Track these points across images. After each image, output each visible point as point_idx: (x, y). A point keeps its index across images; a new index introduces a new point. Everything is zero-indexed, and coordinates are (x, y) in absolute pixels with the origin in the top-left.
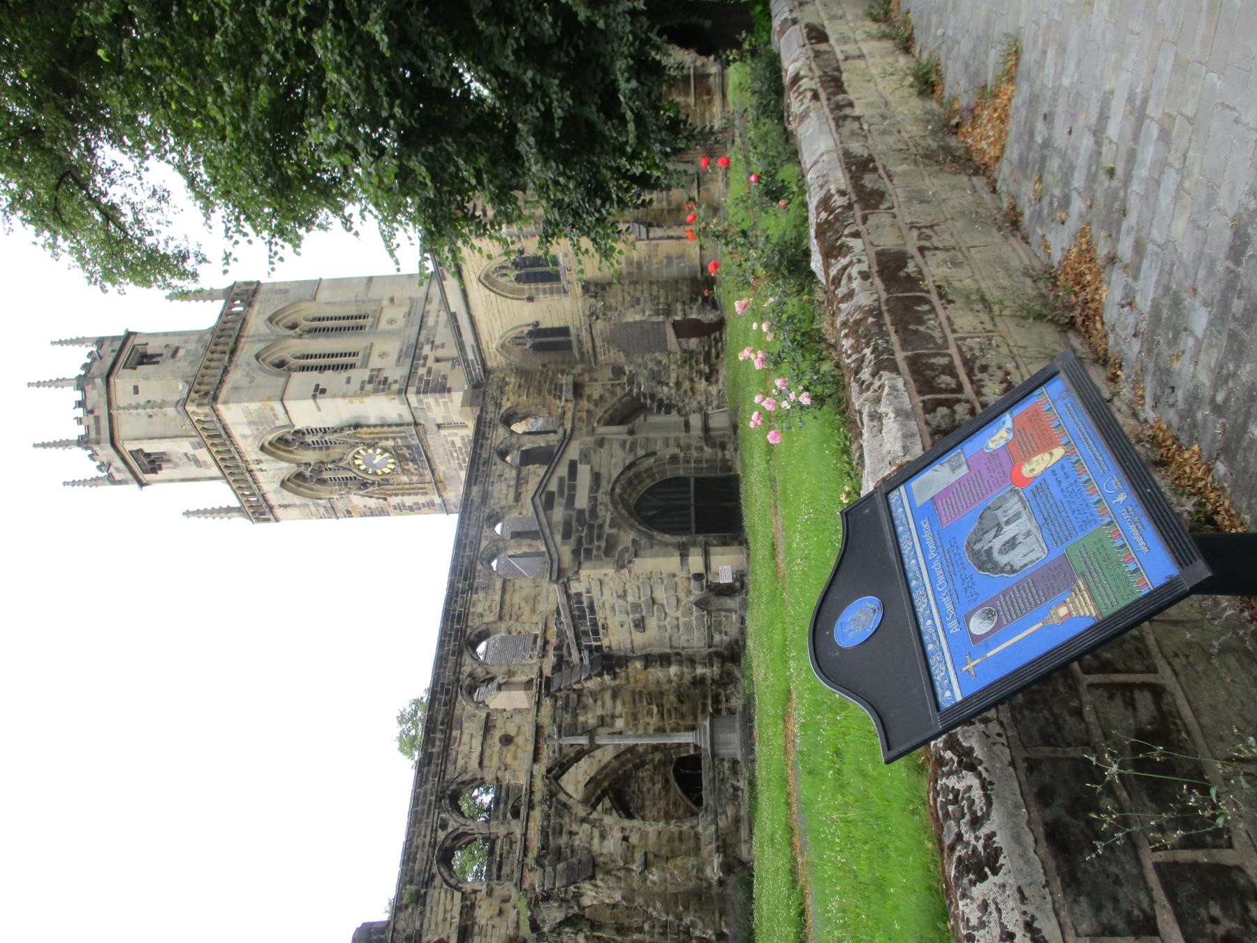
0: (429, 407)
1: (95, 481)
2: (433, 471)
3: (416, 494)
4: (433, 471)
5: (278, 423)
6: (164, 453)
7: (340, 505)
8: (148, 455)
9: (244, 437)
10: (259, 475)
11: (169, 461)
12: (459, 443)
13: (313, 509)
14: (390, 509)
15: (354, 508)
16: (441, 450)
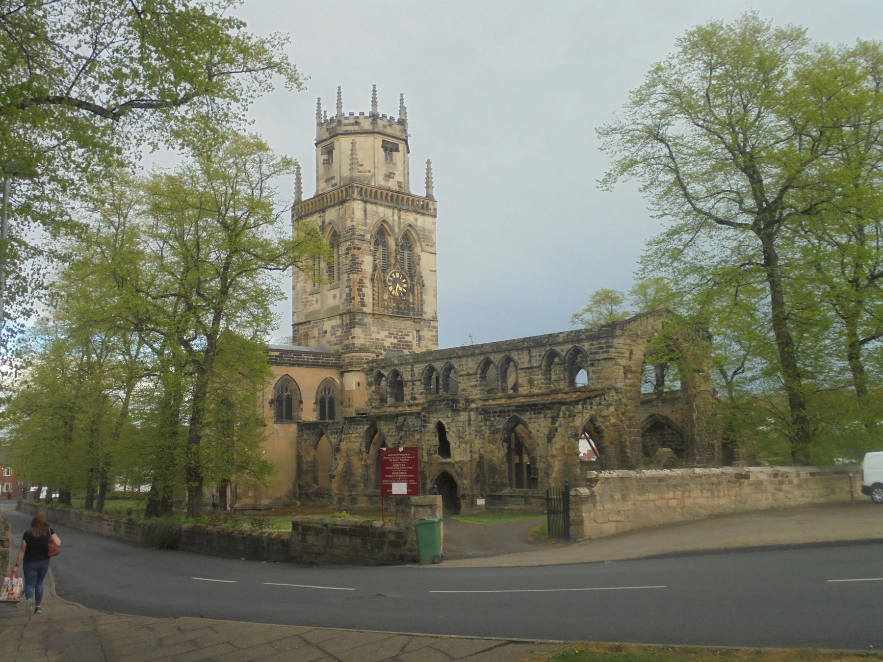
0: (430, 331)
1: (374, 103)
2: (391, 317)
3: (374, 299)
4: (391, 317)
5: (423, 244)
6: (391, 160)
7: (365, 246)
8: (391, 151)
9: (416, 220)
10: (389, 211)
11: (386, 159)
12: (407, 338)
13: (363, 228)
14: (360, 277)
15: (362, 253)
16: (403, 326)
